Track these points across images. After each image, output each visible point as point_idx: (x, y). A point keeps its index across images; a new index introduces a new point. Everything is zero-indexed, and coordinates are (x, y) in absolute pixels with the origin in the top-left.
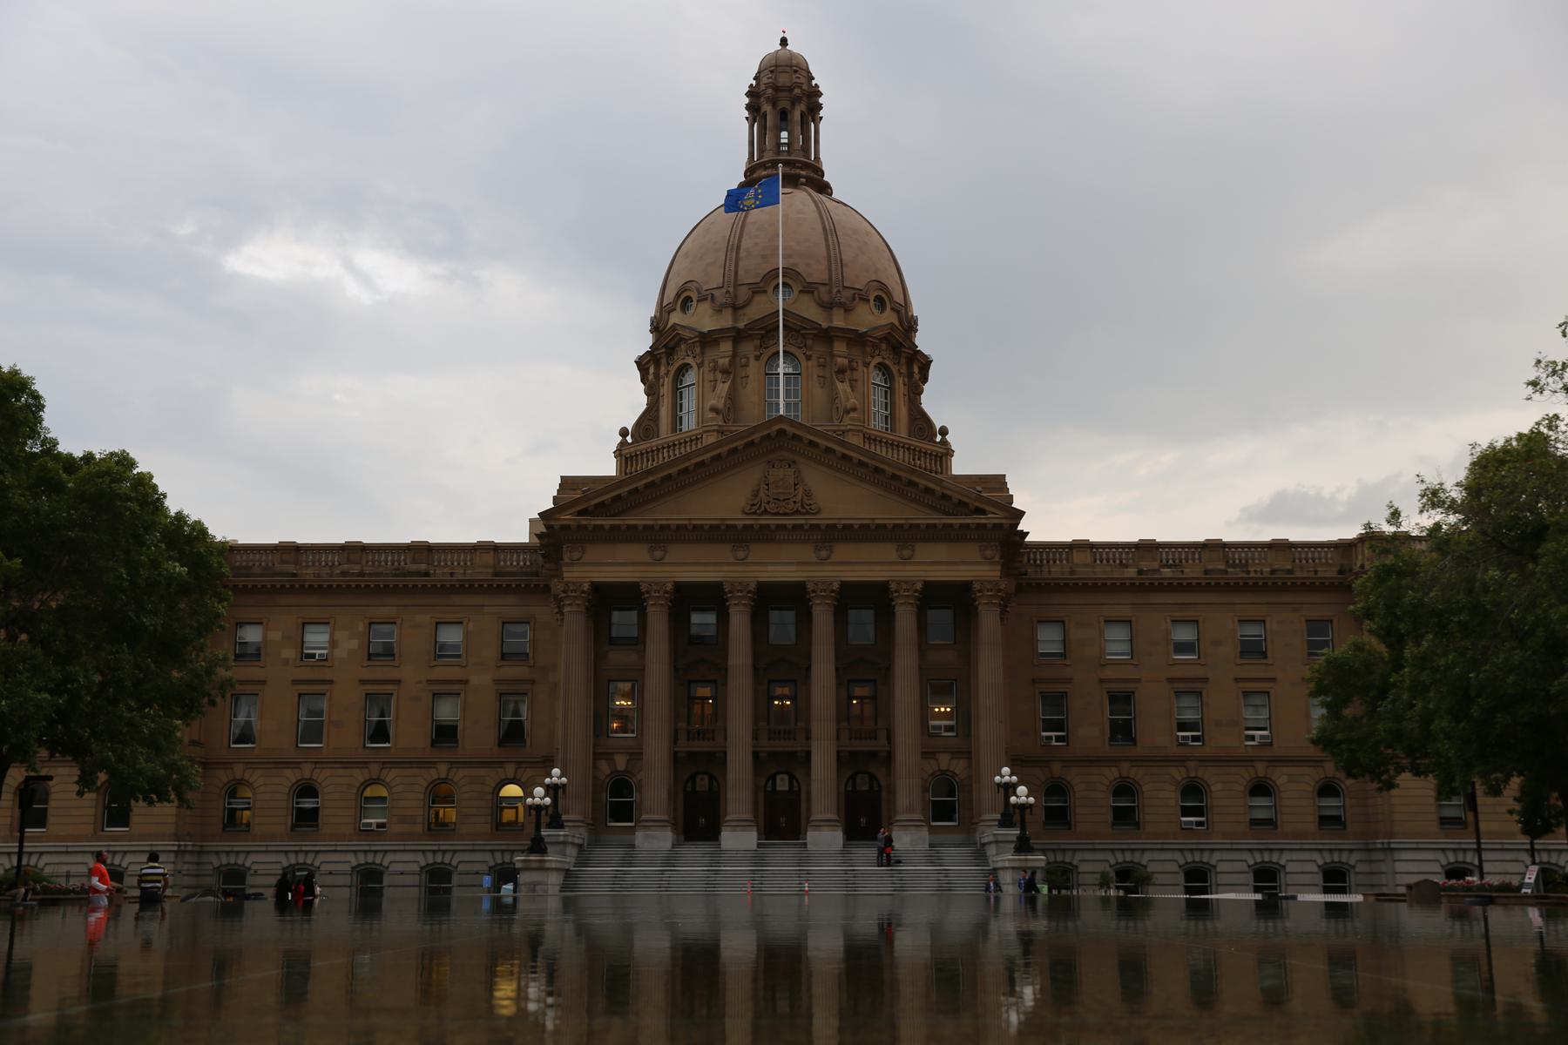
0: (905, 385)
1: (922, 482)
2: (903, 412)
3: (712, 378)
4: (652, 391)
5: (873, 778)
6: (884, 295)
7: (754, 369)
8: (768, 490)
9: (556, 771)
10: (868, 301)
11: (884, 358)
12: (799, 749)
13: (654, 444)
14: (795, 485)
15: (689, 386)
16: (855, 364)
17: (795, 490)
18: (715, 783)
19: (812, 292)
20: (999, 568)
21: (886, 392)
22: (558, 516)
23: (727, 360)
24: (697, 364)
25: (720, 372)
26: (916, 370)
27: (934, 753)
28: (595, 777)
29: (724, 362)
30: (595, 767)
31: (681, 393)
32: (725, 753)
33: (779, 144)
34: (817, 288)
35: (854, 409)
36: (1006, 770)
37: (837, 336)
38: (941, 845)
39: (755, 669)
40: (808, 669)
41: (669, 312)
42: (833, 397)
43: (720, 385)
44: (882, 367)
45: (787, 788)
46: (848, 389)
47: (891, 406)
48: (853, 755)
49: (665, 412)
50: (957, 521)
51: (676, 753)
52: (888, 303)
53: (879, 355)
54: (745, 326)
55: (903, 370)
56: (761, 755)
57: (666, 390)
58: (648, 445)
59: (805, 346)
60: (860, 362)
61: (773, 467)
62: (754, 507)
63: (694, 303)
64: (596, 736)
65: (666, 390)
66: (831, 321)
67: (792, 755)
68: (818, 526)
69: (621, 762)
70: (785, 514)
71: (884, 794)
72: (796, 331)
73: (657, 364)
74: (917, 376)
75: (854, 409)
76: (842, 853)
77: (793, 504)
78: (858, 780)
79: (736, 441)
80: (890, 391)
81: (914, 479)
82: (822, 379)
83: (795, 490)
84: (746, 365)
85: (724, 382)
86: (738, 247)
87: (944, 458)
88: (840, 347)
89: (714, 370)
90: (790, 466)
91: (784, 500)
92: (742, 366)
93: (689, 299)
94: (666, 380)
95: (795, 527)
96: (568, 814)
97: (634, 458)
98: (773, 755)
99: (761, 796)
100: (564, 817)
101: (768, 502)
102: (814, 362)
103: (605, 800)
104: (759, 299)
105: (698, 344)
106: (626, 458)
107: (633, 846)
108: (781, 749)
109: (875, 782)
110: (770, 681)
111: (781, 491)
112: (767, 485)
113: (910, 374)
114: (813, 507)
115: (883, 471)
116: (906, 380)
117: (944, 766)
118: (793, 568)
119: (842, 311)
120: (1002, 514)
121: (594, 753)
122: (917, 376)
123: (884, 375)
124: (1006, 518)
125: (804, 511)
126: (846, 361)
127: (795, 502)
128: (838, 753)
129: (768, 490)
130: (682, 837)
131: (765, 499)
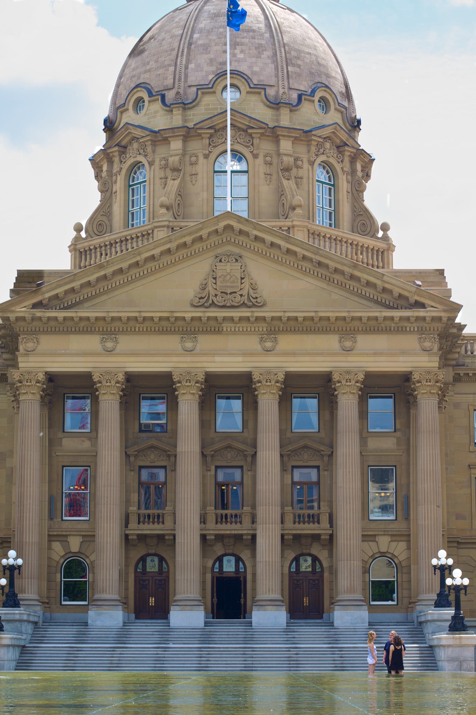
0: (348, 182)
1: (365, 277)
3: (162, 175)
5: (315, 559)
6: (328, 96)
7: (202, 166)
8: (215, 284)
9: (12, 553)
10: (313, 101)
11: (327, 157)
12: (245, 532)
13: (107, 238)
14: (242, 279)
15: (140, 183)
16: (299, 163)
17: (242, 283)
18: (164, 565)
19: (260, 93)
20: (438, 359)
21: (330, 189)
22: (13, 309)
23: (177, 158)
24: (149, 163)
25: (171, 170)
26: (359, 167)
27: (375, 536)
28: (49, 558)
29: (174, 160)
31: (133, 190)
32: (174, 536)
34: (265, 89)
35: (300, 206)
36: (442, 553)
37: (284, 136)
38: (380, 623)
39: (203, 455)
40: (254, 455)
41: (122, 113)
42: (280, 193)
43: (170, 182)
44: (327, 166)
45: (156, 569)
46: (294, 186)
47: (334, 203)
48: (297, 537)
49: (118, 209)
50: (397, 314)
51: (127, 536)
52: (332, 103)
53: (323, 154)
54: (194, 125)
55: (347, 168)
56: (208, 537)
57: (119, 185)
58: (102, 240)
59: (252, 144)
60: (305, 160)
61: (220, 261)
62: (201, 300)
63: (146, 103)
64: (51, 518)
65: (119, 185)
66: (278, 121)
67: (238, 538)
68: (264, 319)
69: (75, 544)
70: (233, 307)
71: (326, 575)
72: (245, 131)
73: (111, 162)
74: (360, 174)
75: (300, 206)
76: (287, 631)
77: (239, 297)
78: (301, 561)
79: (185, 236)
80: (333, 187)
81: (357, 273)
82: (269, 176)
83: (242, 283)
84: (196, 163)
85: (174, 180)
87: (385, 253)
88: (286, 145)
89: (165, 167)
90: (237, 260)
91: (231, 293)
92: (192, 164)
93: (140, 100)
94: (119, 178)
95: (241, 319)
96: (25, 593)
97: (88, 252)
98: (220, 538)
99: (209, 577)
100: (20, 596)
101: (216, 295)
102: (260, 160)
103: (59, 580)
104: (207, 100)
105: (150, 143)
106: (81, 253)
107: (86, 624)
108: (228, 532)
109: (241, 564)
110: (217, 467)
111: (229, 284)
112: (215, 279)
113: (353, 171)
114: (259, 300)
115: (327, 266)
116: (349, 177)
118: (240, 359)
119: (288, 110)
120: (440, 307)
121: (49, 535)
122: (360, 174)
123: (328, 172)
124: (445, 311)
125: (251, 304)
126: (291, 160)
127: (241, 295)
128: (282, 536)
129: (215, 284)
130: (133, 616)
131: (213, 292)
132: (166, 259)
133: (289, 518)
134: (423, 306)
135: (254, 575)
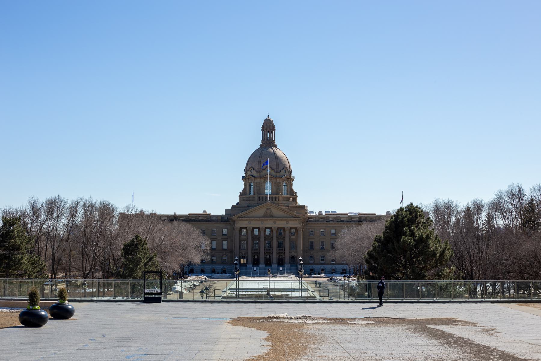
2: (289, 190)
4: (245, 185)
5: (282, 256)
30: (239, 254)
33: (267, 137)
36: (301, 257)
40: (272, 239)
44: (286, 183)
50: (295, 219)
51: (252, 252)
55: (289, 182)
57: (248, 185)
65: (248, 185)
67: (270, 253)
71: (284, 259)
86: (261, 162)
113: (290, 182)
117: (293, 254)
132: (259, 209)
133: (278, 250)
134: (299, 218)
135: (272, 259)
